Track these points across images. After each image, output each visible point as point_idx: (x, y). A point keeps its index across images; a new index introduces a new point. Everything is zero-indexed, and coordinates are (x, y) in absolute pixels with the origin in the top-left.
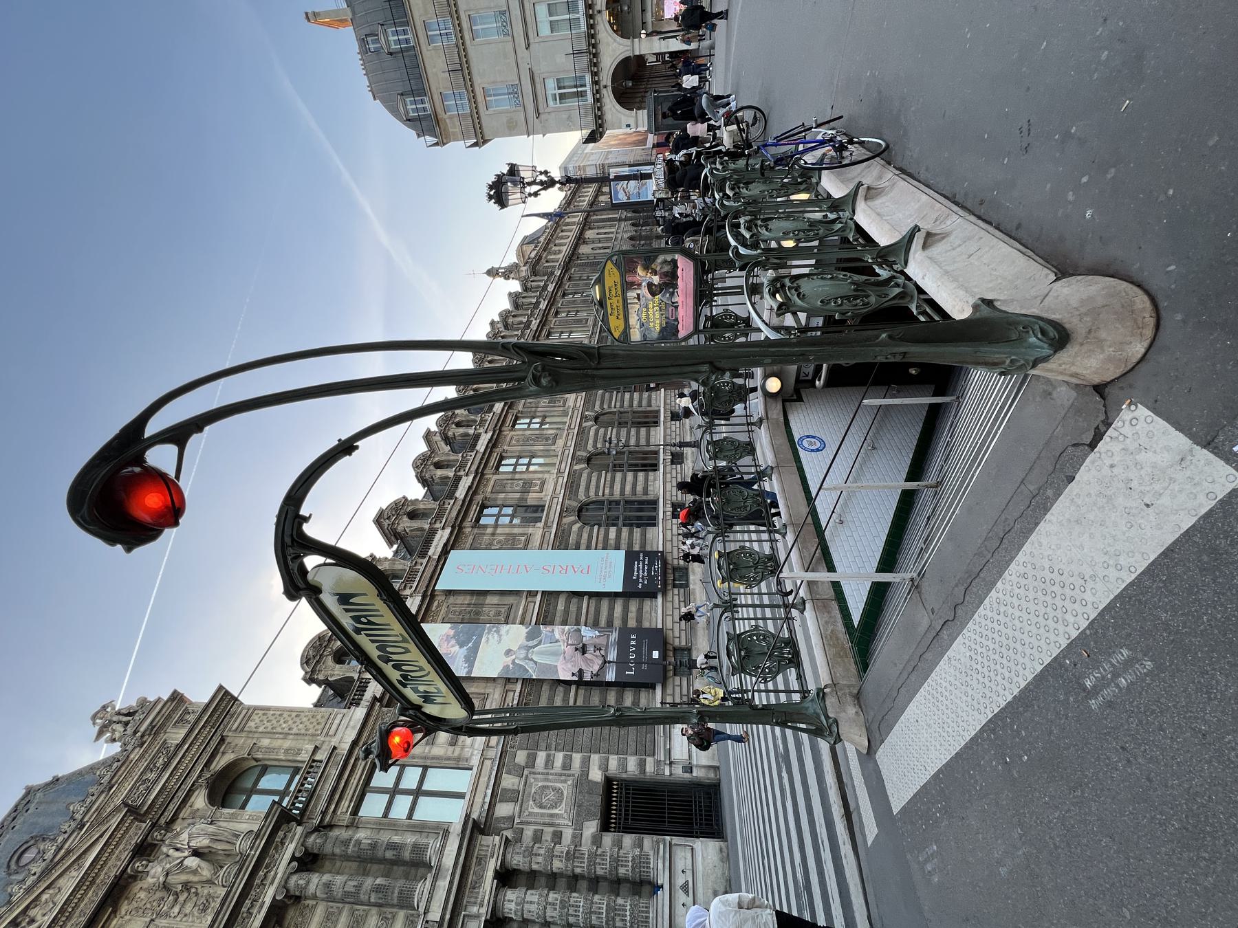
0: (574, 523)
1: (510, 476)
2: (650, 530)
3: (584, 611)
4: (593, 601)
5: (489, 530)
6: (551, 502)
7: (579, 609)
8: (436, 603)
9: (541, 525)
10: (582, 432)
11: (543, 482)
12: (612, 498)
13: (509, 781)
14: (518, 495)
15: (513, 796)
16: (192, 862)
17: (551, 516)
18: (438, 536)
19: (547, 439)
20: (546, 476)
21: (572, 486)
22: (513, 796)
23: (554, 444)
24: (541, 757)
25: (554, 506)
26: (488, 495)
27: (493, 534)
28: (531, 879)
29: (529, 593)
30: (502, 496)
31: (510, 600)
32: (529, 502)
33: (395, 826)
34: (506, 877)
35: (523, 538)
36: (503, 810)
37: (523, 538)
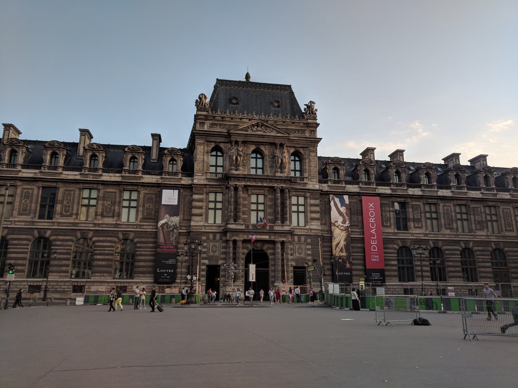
0: (398, 245)
1: (422, 211)
2: (397, 278)
3: (358, 254)
4: (362, 257)
5: (391, 209)
6: (409, 233)
7: (358, 252)
8: (357, 197)
9: (396, 231)
10: (457, 242)
11: (421, 228)
12: (414, 262)
13: (303, 238)
14: (411, 217)
15: (299, 240)
16: (280, 160)
17: (401, 235)
18: (387, 188)
19: (449, 225)
20: (424, 228)
21: (418, 242)
22: (299, 240)
23: (446, 228)
24: (309, 247)
25: (407, 235)
26: (410, 204)
27: (390, 211)
28: (283, 249)
29: (363, 232)
30: (411, 210)
31: (360, 225)
32: (408, 223)
33: (290, 208)
34: (283, 243)
35: (389, 224)
36: (296, 238)
37: (389, 224)
